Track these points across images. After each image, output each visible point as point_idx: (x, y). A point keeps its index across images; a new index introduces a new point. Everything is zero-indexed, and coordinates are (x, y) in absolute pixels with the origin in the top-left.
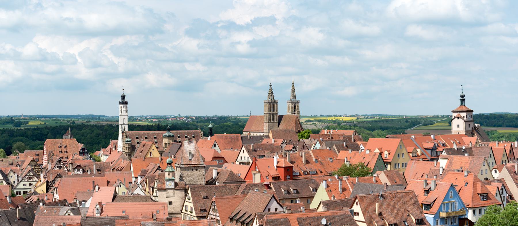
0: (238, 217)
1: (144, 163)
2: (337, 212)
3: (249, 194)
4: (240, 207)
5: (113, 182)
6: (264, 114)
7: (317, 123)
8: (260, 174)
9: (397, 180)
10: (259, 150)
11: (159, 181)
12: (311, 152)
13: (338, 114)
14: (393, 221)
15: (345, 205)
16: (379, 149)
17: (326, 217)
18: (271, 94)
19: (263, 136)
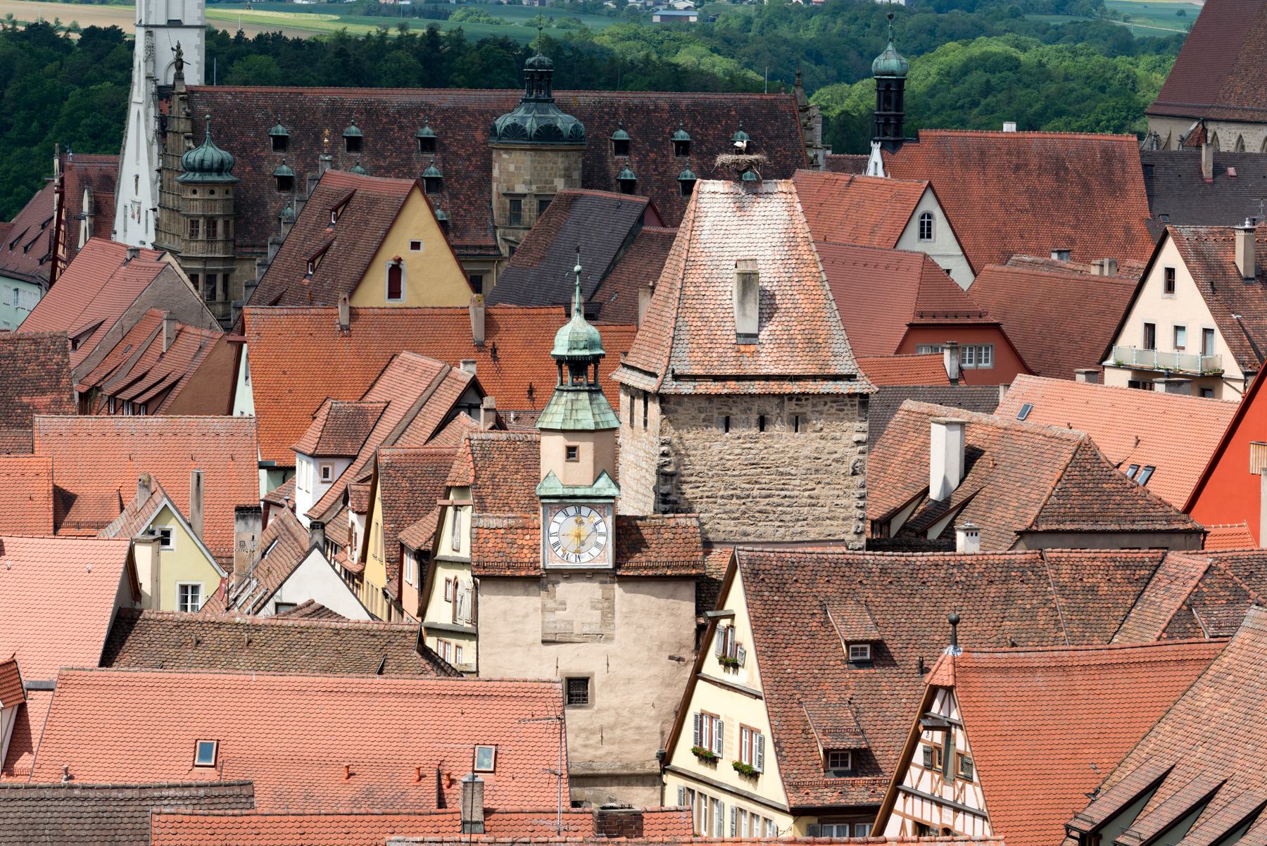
1: (345, 348)
4: (1164, 744)
5: (103, 502)
11: (481, 507)
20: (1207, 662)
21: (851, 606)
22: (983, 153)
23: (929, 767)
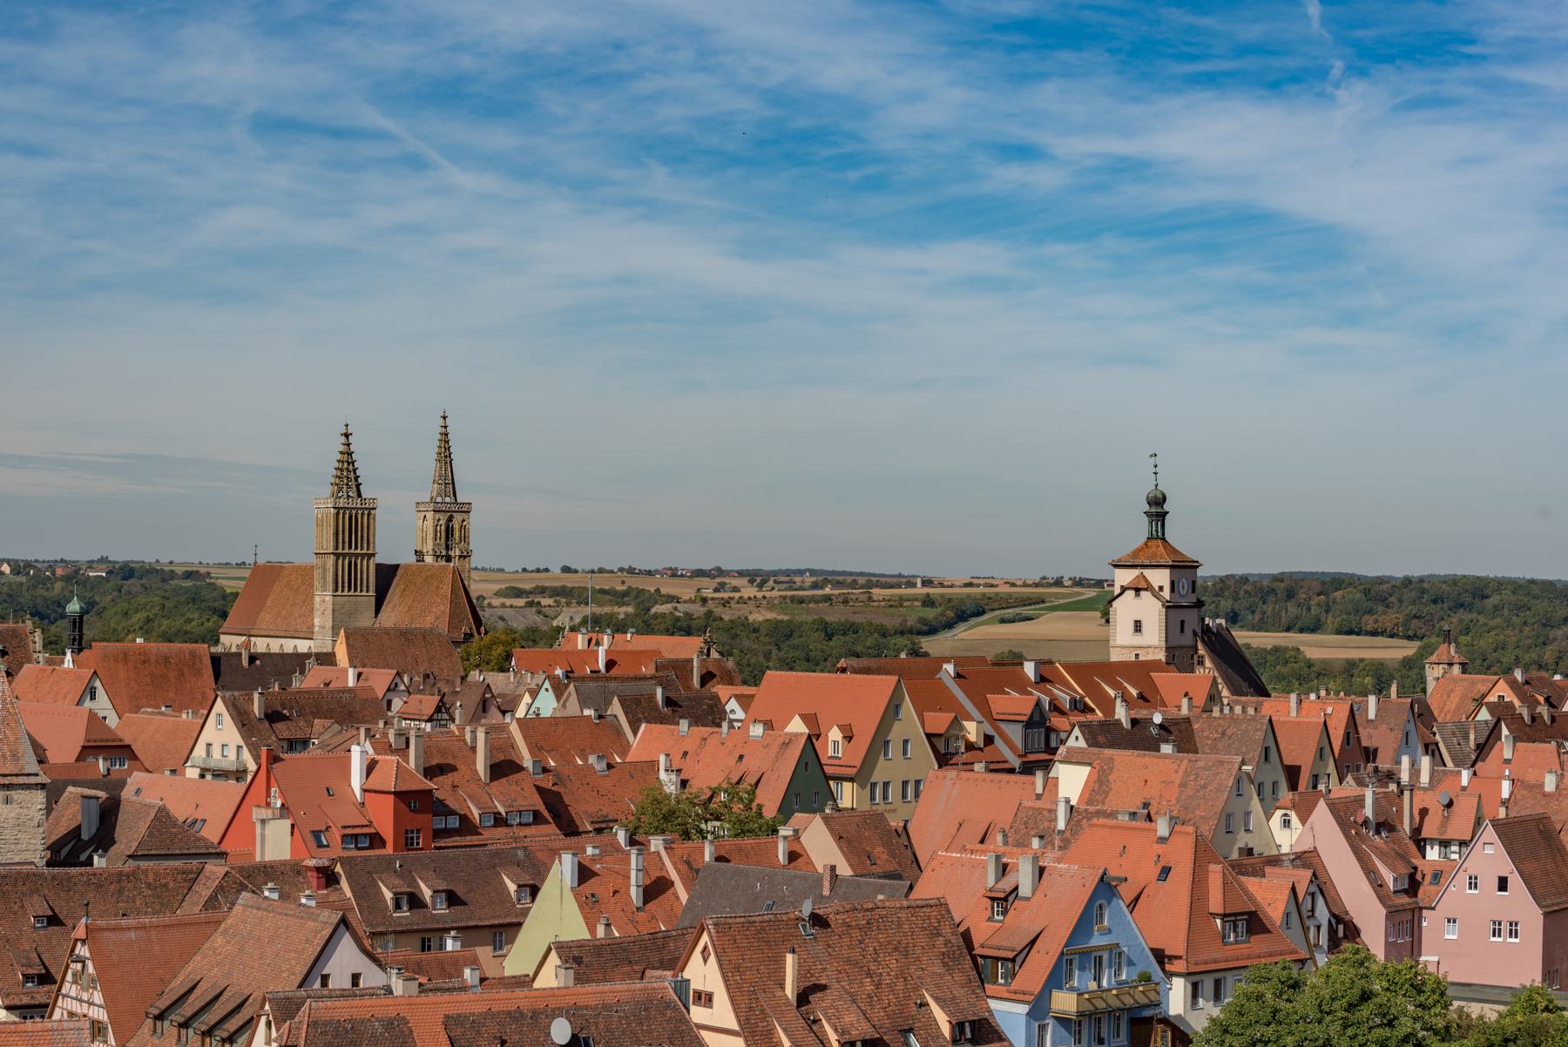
0: (188, 1009)
2: (619, 989)
3: (238, 908)
6: (313, 560)
7: (546, 601)
8: (287, 823)
9: (880, 853)
10: (285, 716)
12: (515, 729)
13: (640, 565)
14: (861, 1029)
15: (655, 958)
16: (804, 718)
17: (572, 1013)
18: (347, 473)
19: (307, 656)
20: (219, 923)
21: (36, 897)
22: (126, 655)
23: (75, 982)
